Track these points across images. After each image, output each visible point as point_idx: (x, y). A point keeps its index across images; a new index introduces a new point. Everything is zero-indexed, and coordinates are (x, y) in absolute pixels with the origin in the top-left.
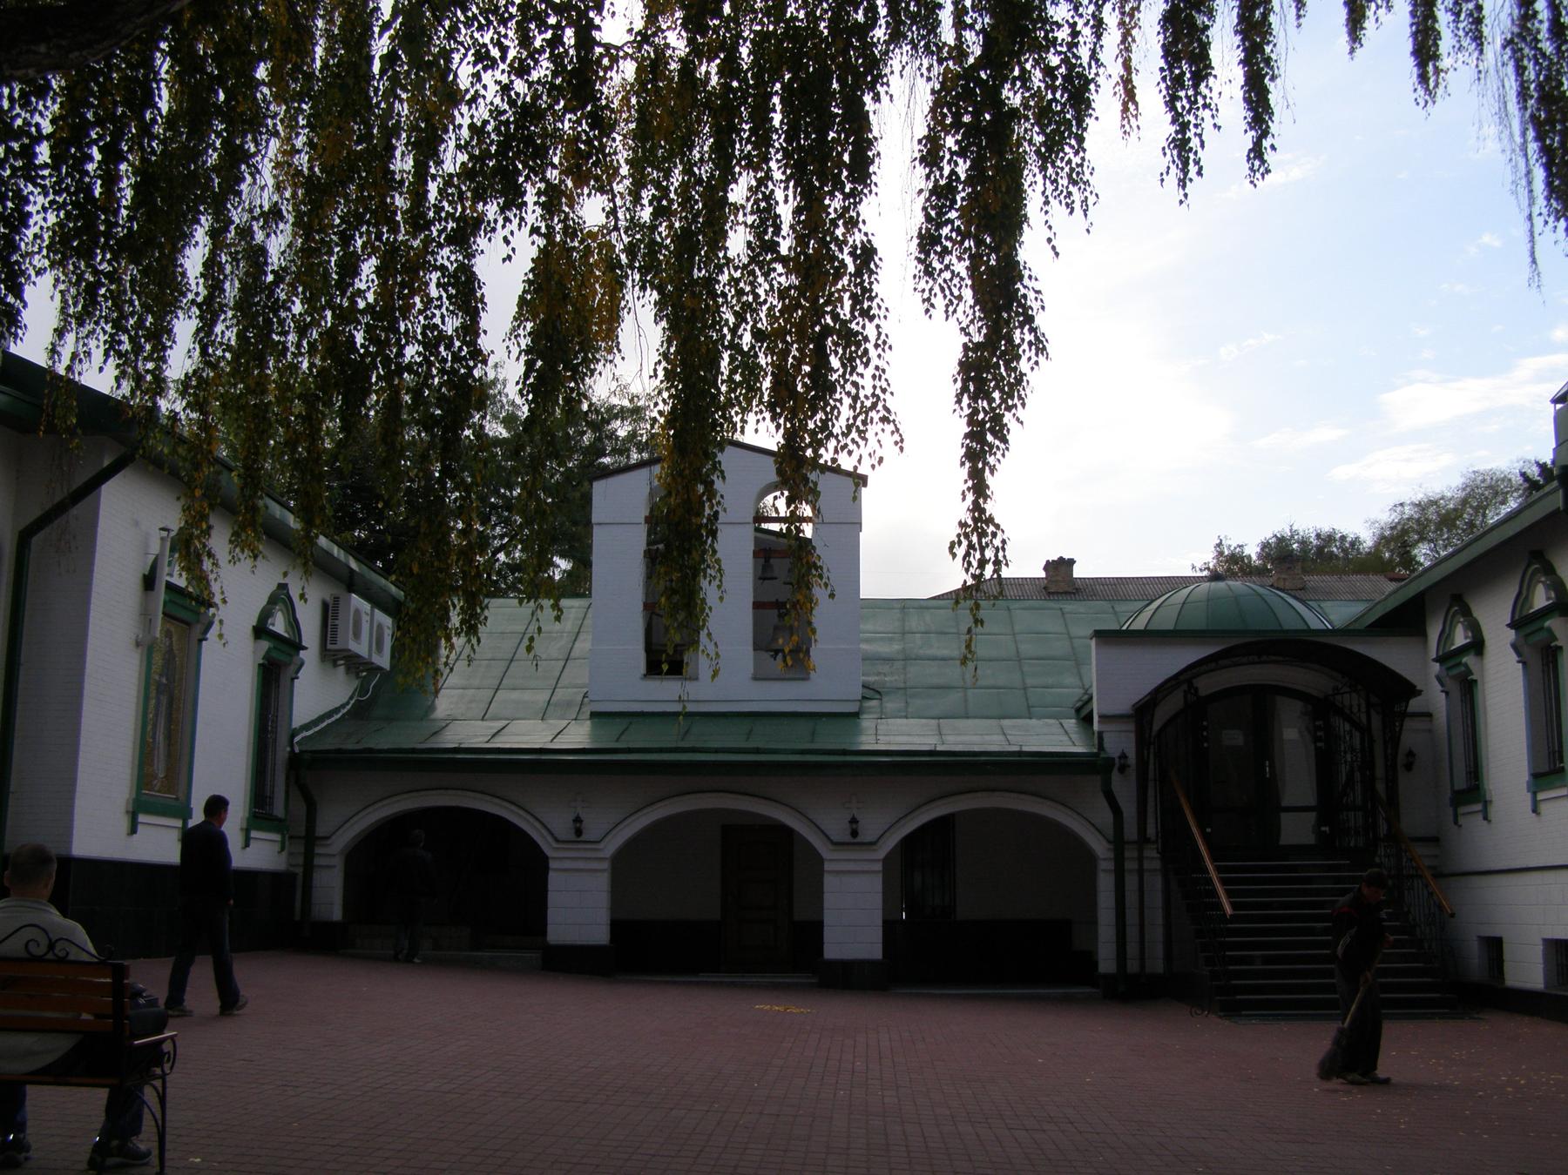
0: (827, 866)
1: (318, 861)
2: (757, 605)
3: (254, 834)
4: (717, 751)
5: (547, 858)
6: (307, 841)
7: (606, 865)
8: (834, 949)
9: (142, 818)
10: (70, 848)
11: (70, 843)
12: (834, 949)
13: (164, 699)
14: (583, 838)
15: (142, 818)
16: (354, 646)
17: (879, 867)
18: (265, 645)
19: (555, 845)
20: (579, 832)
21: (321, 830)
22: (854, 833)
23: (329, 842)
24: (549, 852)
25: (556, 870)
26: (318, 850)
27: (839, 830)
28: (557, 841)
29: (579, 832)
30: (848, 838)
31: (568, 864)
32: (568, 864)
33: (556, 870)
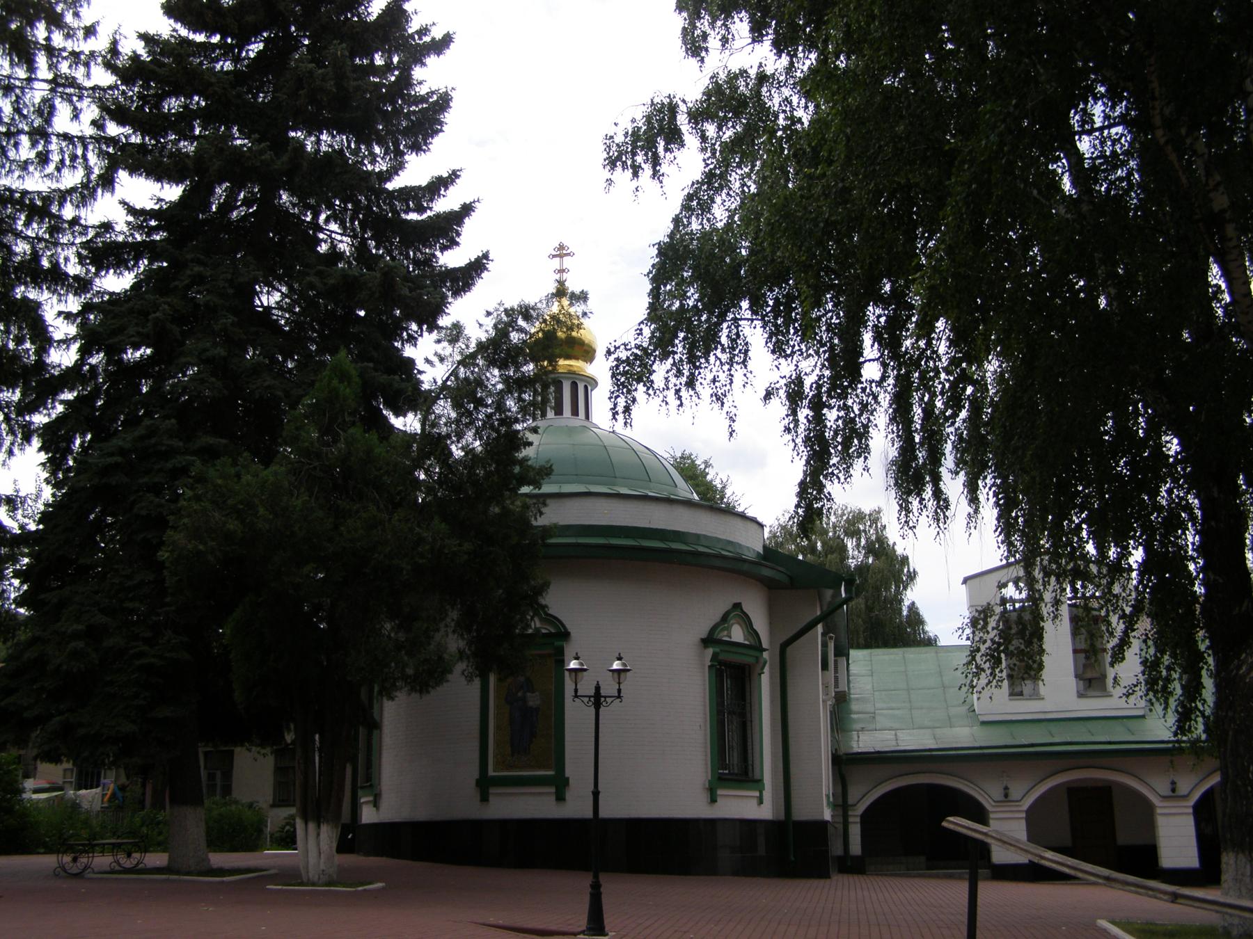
0: (1159, 811)
2: (1075, 651)
4: (1084, 743)
5: (988, 811)
7: (1024, 815)
14: (1010, 798)
17: (1191, 810)
19: (993, 804)
20: (1006, 796)
21: (850, 801)
22: (1173, 790)
23: (855, 808)
25: (993, 819)
26: (850, 813)
27: (1164, 789)
28: (994, 801)
29: (1006, 796)
30: (1171, 794)
33: (993, 819)
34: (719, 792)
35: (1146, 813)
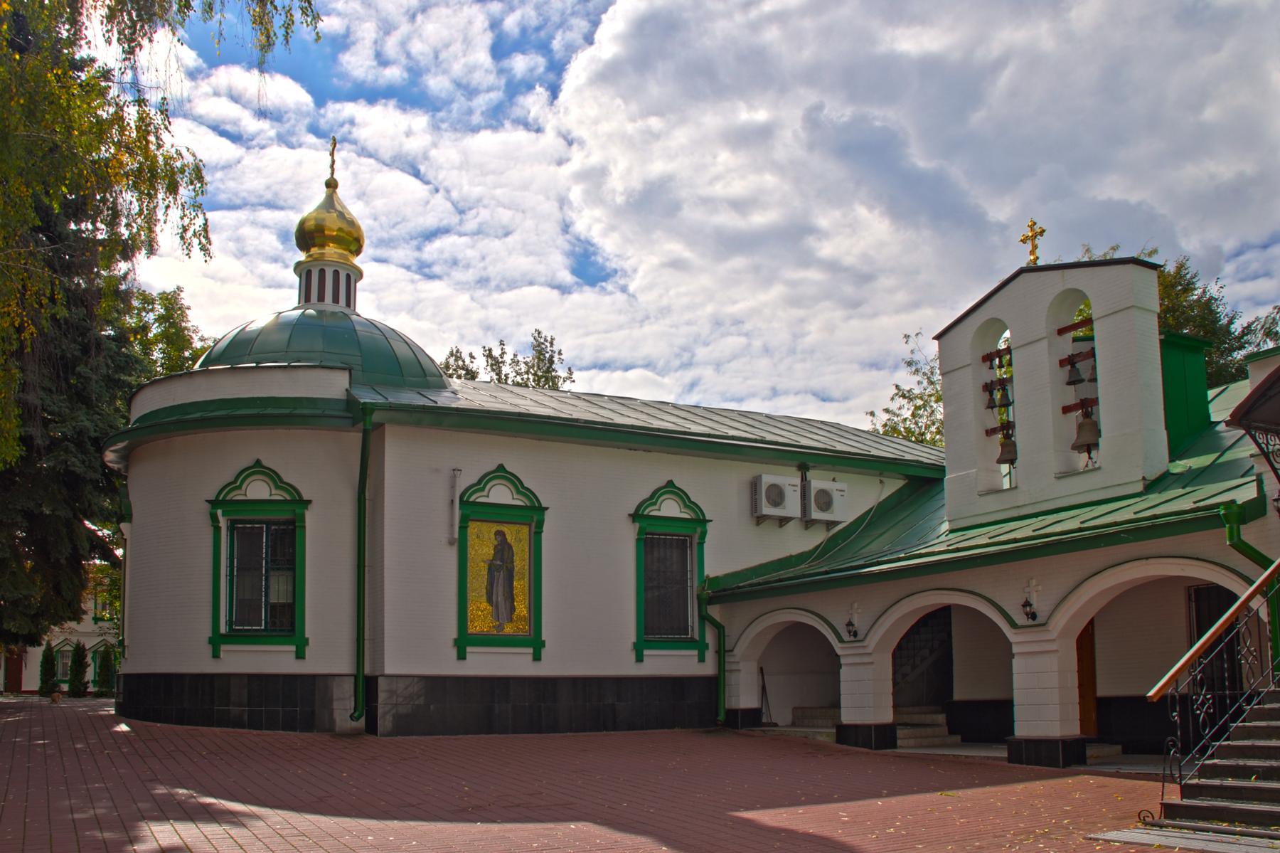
1: (727, 667)
3: (646, 652)
6: (722, 653)
8: (1022, 729)
9: (469, 649)
10: (384, 670)
11: (383, 667)
12: (1022, 729)
13: (501, 577)
15: (469, 649)
16: (767, 510)
18: (637, 525)
24: (839, 652)
26: (727, 659)
29: (855, 634)
31: (850, 660)
32: (850, 660)
34: (224, 647)
35: (1005, 651)
